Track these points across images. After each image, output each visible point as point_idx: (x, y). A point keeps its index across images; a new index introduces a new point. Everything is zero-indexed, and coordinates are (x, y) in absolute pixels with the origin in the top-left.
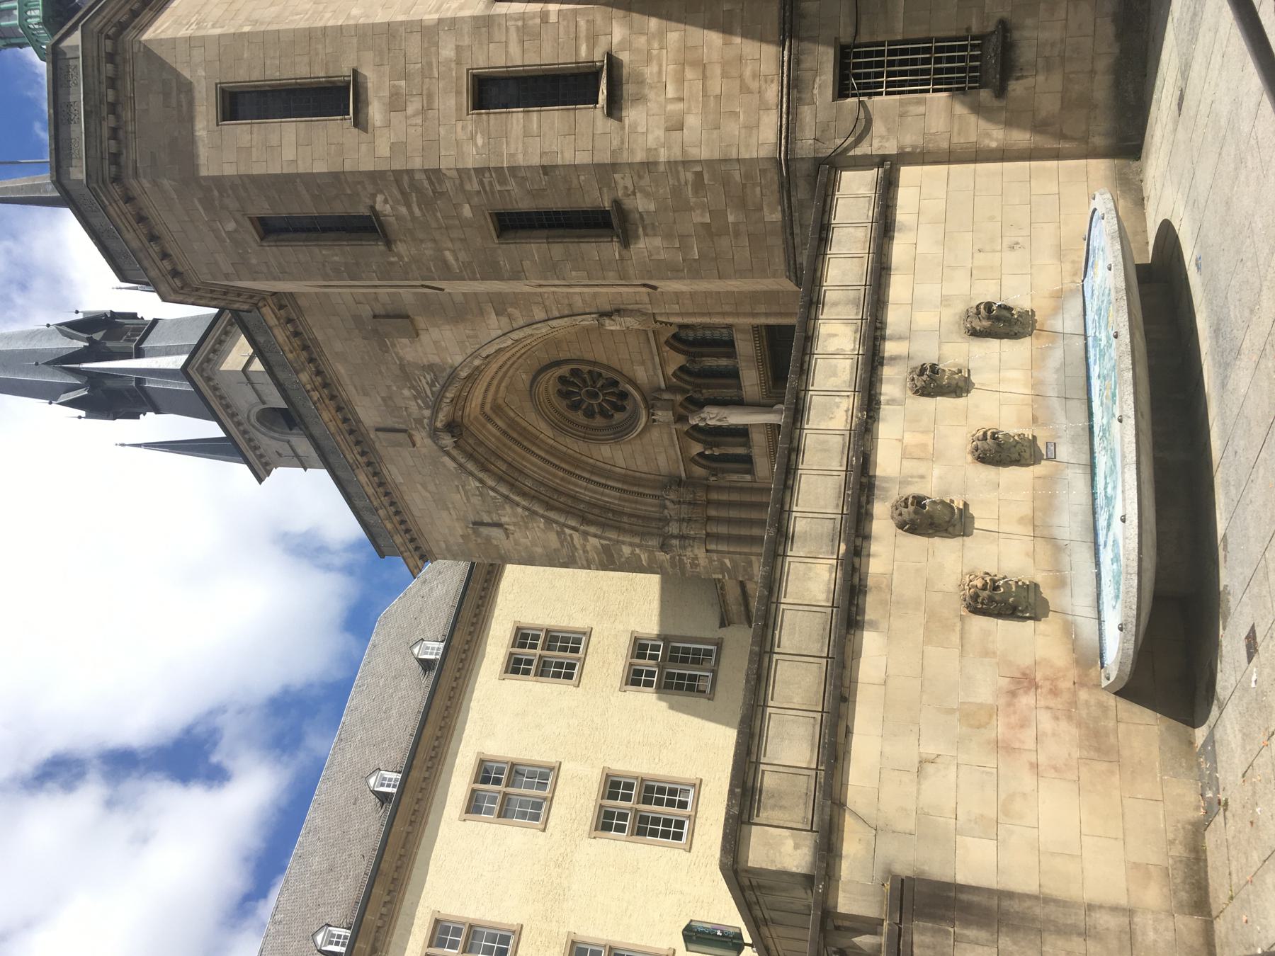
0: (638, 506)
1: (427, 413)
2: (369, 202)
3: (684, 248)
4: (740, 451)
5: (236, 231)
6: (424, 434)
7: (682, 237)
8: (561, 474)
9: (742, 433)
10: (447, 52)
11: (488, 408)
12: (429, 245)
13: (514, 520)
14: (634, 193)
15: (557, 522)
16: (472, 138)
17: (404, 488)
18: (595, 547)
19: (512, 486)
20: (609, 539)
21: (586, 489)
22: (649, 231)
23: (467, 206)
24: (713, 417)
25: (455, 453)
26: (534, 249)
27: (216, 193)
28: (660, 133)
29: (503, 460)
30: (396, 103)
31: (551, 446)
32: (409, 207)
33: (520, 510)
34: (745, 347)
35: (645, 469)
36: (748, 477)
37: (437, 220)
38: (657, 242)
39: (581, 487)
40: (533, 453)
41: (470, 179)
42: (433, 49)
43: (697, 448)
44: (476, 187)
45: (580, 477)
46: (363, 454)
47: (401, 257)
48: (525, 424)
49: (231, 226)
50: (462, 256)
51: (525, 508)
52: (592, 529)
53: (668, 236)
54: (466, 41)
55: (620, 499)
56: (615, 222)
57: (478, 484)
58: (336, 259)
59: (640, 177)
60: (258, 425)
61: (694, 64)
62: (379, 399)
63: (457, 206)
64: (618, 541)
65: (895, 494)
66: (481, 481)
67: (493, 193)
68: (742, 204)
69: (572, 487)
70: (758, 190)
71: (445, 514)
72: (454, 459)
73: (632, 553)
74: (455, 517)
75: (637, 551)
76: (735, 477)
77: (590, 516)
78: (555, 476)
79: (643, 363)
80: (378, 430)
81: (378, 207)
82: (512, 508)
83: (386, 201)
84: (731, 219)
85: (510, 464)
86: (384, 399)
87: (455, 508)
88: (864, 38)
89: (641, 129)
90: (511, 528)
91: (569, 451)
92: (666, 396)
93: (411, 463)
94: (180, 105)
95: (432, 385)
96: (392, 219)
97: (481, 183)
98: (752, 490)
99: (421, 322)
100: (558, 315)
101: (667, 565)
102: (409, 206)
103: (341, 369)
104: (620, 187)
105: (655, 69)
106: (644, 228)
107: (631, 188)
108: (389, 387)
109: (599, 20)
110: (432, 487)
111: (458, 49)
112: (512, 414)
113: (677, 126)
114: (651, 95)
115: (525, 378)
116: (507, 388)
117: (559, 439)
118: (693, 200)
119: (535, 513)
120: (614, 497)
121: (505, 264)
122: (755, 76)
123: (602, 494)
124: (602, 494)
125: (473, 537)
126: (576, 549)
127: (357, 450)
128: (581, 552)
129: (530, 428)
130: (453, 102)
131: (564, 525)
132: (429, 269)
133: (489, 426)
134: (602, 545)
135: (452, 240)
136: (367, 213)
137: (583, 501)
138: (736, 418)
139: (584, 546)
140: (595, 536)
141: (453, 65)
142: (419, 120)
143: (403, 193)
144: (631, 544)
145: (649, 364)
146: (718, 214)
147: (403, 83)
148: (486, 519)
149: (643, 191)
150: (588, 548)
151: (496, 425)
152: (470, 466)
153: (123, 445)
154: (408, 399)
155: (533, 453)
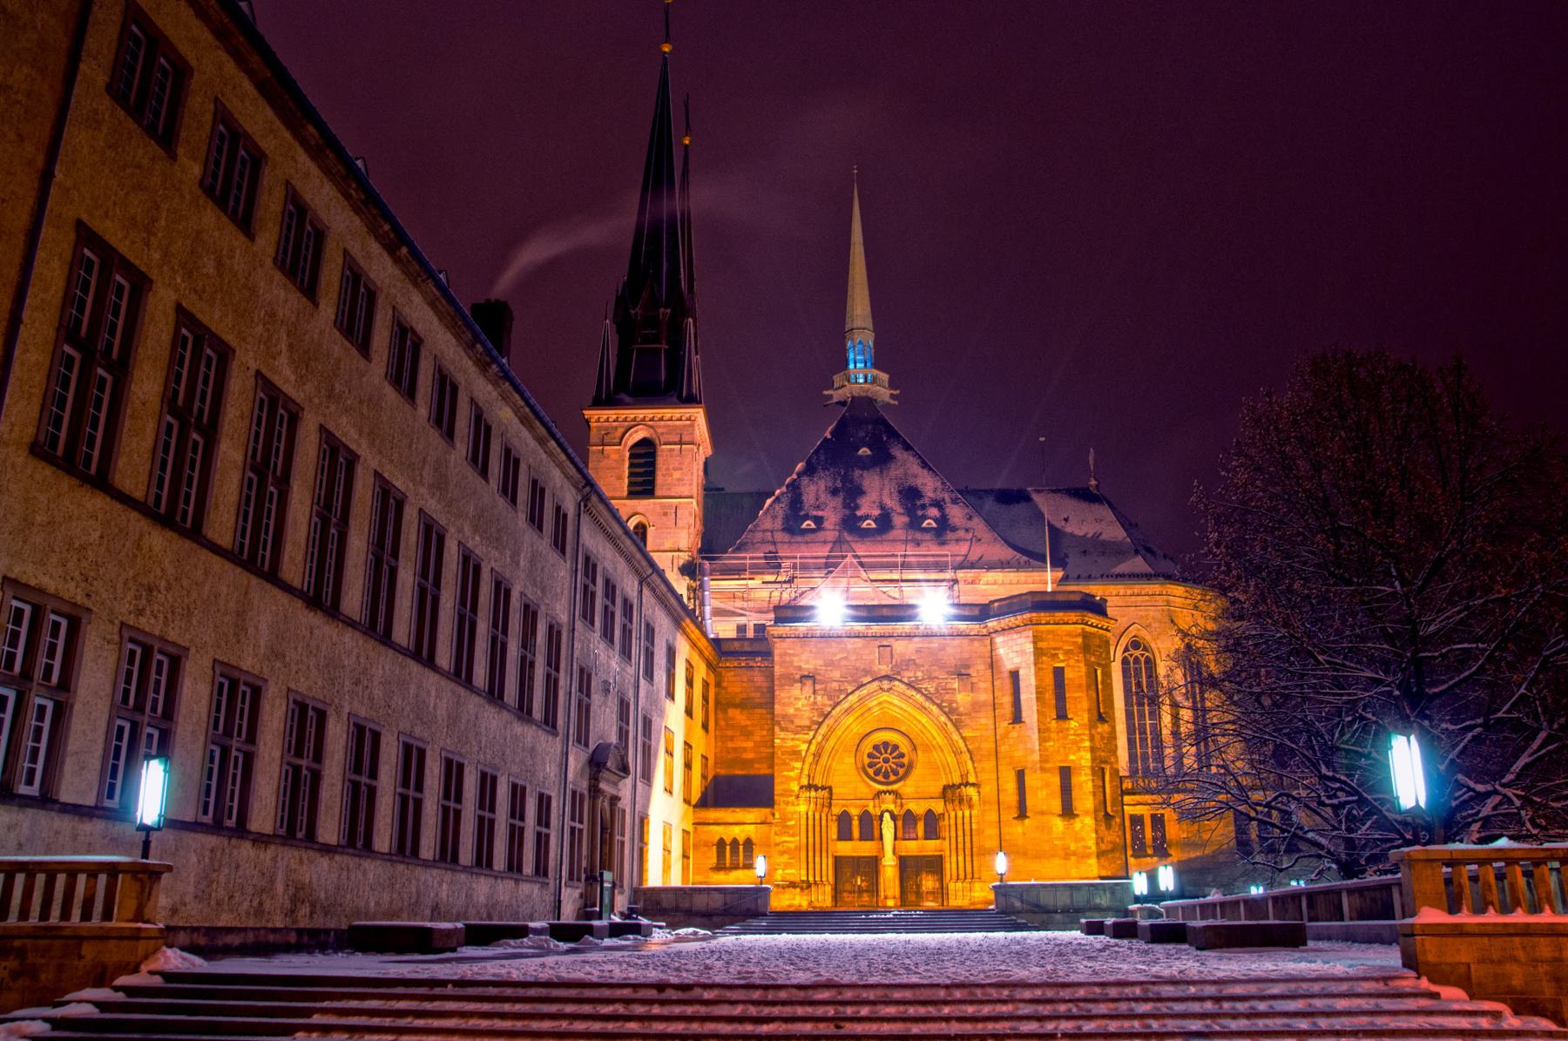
1: (905, 680)
13: (819, 703)
26: (1056, 780)
32: (1074, 735)
33: (829, 709)
34: (930, 847)
49: (1061, 657)
50: (1051, 749)
51: (830, 712)
52: (813, 748)
53: (1064, 833)
57: (849, 691)
63: (1074, 754)
71: (821, 662)
95: (926, 689)
101: (785, 786)
108: (923, 666)
110: (843, 663)
115: (903, 729)
119: (826, 716)
128: (792, 736)
133: (876, 702)
144: (802, 769)
148: (818, 687)
150: (797, 742)
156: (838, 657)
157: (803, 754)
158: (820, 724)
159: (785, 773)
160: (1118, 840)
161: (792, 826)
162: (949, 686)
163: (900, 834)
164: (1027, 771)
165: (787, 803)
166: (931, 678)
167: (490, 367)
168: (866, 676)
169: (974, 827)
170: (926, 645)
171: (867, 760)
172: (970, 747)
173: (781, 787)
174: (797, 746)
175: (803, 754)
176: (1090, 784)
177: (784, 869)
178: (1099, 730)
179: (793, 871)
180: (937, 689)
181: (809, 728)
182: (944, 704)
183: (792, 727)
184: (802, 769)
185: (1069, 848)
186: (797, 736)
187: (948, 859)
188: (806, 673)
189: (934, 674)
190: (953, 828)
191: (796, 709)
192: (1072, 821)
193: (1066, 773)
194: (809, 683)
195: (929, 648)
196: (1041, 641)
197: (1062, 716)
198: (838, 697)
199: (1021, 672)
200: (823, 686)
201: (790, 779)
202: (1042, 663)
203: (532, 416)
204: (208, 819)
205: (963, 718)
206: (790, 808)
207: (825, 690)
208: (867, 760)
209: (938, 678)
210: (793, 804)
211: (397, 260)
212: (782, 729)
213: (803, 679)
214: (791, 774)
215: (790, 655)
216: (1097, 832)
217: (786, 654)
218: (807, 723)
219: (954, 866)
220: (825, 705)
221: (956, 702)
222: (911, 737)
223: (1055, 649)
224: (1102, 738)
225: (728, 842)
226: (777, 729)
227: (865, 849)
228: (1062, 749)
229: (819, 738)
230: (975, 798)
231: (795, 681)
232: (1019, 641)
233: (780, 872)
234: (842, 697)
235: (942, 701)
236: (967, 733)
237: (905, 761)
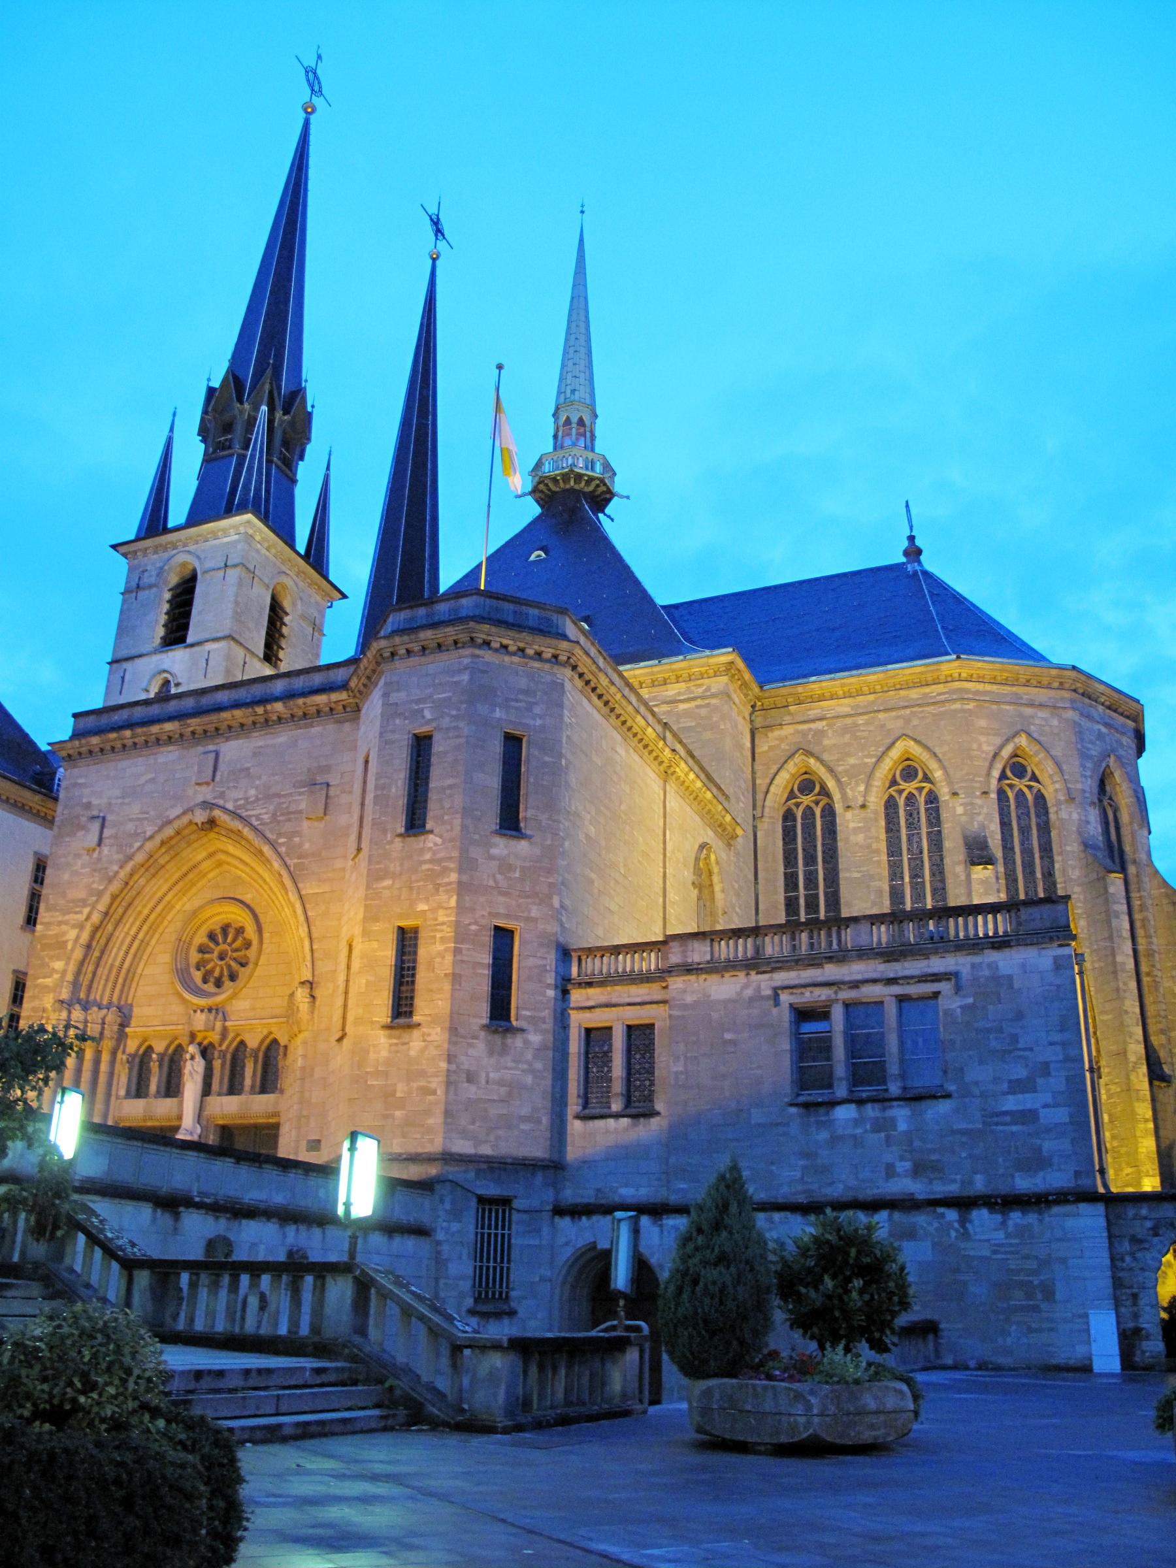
0: (102, 982)
1: (230, 806)
2: (436, 831)
3: (377, 1074)
4: (153, 1088)
5: (423, 717)
7: (386, 1074)
8: (146, 912)
9: (172, 1088)
10: (535, 912)
11: (223, 857)
13: (104, 859)
14: (424, 1041)
15: (97, 901)
16: (476, 923)
17: (151, 760)
18: (64, 934)
20: (73, 950)
21: (127, 933)
22: (394, 1048)
23: (426, 908)
25: (185, 820)
26: (388, 954)
27: (454, 713)
28: (466, 1067)
29: (169, 861)
30: (505, 866)
31: (173, 907)
32: (430, 861)
33: (116, 868)
35: (140, 993)
36: (122, 1092)
37: (417, 881)
38: (384, 1054)
39: (130, 929)
40: (170, 889)
41: (447, 915)
42: (537, 901)
44: (441, 919)
45: (140, 929)
46: (193, 733)
47: (391, 842)
48: (199, 885)
49: (428, 714)
50: (386, 893)
51: (117, 873)
52: (85, 937)
53: (388, 1062)
54: (541, 927)
55: (112, 966)
56: (402, 1021)
57: (149, 834)
58: (394, 790)
59: (436, 1047)
61: (510, 1094)
62: (249, 765)
63: (427, 900)
64: (69, 958)
65: (232, 1237)
66: (151, 837)
67: (436, 930)
69: (131, 920)
70: (418, 1136)
71: (117, 792)
72: (178, 817)
73: (54, 971)
74: (113, 801)
75: (56, 976)
76: (124, 1080)
77: (98, 935)
78: (144, 906)
79: (253, 1009)
80: (217, 754)
81: (431, 836)
83: (436, 844)
84: (398, 1113)
85: (163, 866)
86: (248, 769)
87: (122, 804)
88: (516, 1216)
89: (471, 1052)
90: (95, 855)
91: (165, 923)
92: (218, 1025)
93: (177, 776)
94: (517, 701)
95: (258, 818)
96: (421, 845)
97: (443, 924)
98: (108, 1094)
100: (315, 947)
101: (36, 1003)
102: (430, 861)
104: (430, 1031)
105: (510, 1064)
106: (396, 1044)
107: (429, 1039)
108: (259, 778)
109: (544, 1026)
110: (148, 788)
111: (535, 920)
112: (211, 875)
113: (471, 1078)
114: (492, 1061)
115: (247, 898)
116: (239, 877)
118: (415, 1085)
119: (110, 881)
120: (115, 959)
121: (376, 927)
122: (498, 1138)
123: (119, 949)
124: (119, 949)
125: (89, 814)
126: (64, 914)
127: (199, 729)
128: (60, 919)
129: (194, 890)
130: (502, 911)
131: (93, 908)
132: (378, 863)
133: (204, 854)
134: (67, 941)
135: (401, 888)
136: (428, 827)
137: (115, 929)
138: (191, 1088)
139: (66, 923)
140: (78, 937)
141: (525, 914)
142: (491, 883)
143: (439, 861)
144: (64, 972)
147: (517, 875)
148: (107, 832)
149: (426, 1047)
150: (64, 928)
151: (204, 859)
152: (169, 831)
153: (174, 415)
154: (246, 792)
155: (170, 889)
158: (100, 894)
159: (41, 981)
160: (529, 1080)
162: (293, 808)
166: (268, 797)
168: (172, 807)
170: (270, 742)
171: (194, 957)
176: (449, 958)
178: (494, 851)
180: (274, 815)
181: (84, 903)
182: (281, 840)
186: (67, 917)
189: (273, 790)
191: (76, 873)
192: (406, 1036)
193: (407, 941)
196: (398, 690)
197: (415, 822)
198: (131, 846)
201: (46, 989)
202: (393, 731)
208: (194, 957)
209: (278, 796)
214: (48, 981)
215: (80, 784)
216: (450, 1058)
217: (75, 785)
218: (81, 894)
221: (297, 833)
222: (258, 910)
223: (417, 702)
228: (405, 892)
234: (137, 845)
235: (280, 835)
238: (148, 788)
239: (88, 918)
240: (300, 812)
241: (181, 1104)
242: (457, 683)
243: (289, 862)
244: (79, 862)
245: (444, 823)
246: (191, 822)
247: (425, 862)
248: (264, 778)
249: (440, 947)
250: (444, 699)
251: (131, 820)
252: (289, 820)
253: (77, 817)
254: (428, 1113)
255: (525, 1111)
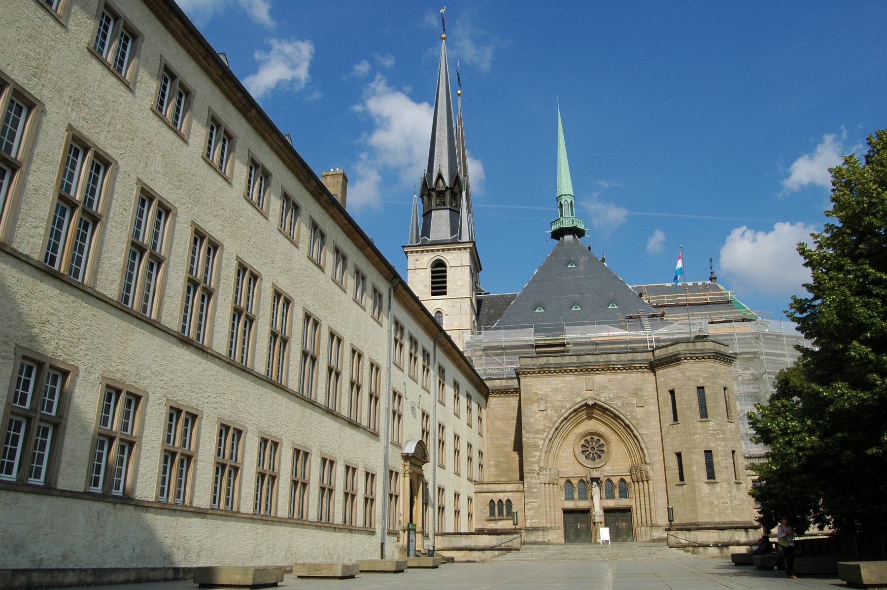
1: (603, 399)
6: (592, 395)
7: (709, 497)
12: (701, 432)
13: (549, 415)
15: (550, 430)
17: (562, 378)
18: (538, 442)
19: (566, 418)
24: (596, 490)
25: (584, 402)
26: (703, 460)
33: (556, 419)
34: (623, 503)
36: (562, 499)
38: (707, 491)
43: (575, 482)
50: (698, 440)
52: (547, 442)
53: (709, 494)
57: (568, 407)
60: (436, 258)
63: (713, 442)
68: (720, 513)
71: (549, 390)
82: (556, 416)
84: (716, 510)
92: (602, 476)
93: (576, 386)
95: (616, 404)
99: (643, 409)
101: (530, 467)
103: (620, 376)
108: (613, 390)
110: (563, 389)
117: (573, 435)
118: (720, 501)
119: (555, 423)
121: (697, 450)
126: (535, 435)
131: (549, 433)
139: (538, 438)
140: (544, 443)
143: (716, 430)
144: (540, 456)
145: (613, 471)
146: (717, 506)
148: (548, 405)
150: (537, 440)
152: (577, 406)
156: (560, 386)
157: (541, 447)
158: (551, 428)
160: (745, 498)
161: (536, 492)
162: (630, 402)
163: (604, 496)
164: (682, 454)
165: (532, 478)
166: (619, 398)
167: (322, 197)
169: (651, 490)
172: (645, 440)
173: (527, 468)
174: (537, 442)
175: (541, 447)
177: (531, 520)
178: (728, 427)
179: (537, 521)
180: (622, 404)
181: (544, 431)
182: (628, 414)
183: (533, 430)
184: (540, 456)
185: (713, 503)
186: (537, 436)
187: (635, 512)
188: (540, 397)
189: (620, 395)
190: (637, 491)
191: (535, 419)
192: (714, 486)
194: (543, 402)
195: (616, 379)
196: (688, 371)
199: (676, 392)
200: (551, 404)
201: (534, 463)
202: (689, 385)
203: (354, 231)
204: (99, 489)
205: (640, 422)
206: (534, 481)
207: (553, 407)
210: (536, 479)
211: (249, 120)
212: (527, 432)
213: (539, 401)
217: (528, 385)
218: (542, 427)
219: (639, 515)
220: (553, 416)
223: (697, 376)
224: (731, 432)
225: (496, 503)
226: (523, 432)
227: (583, 504)
229: (550, 436)
230: (650, 473)
231: (536, 402)
232: (674, 372)
233: (529, 521)
234: (564, 411)
235: (627, 412)
236: (642, 431)
237: (605, 449)
238: (563, 389)
239: (547, 437)
240: (634, 404)
241: (600, 504)
242: (710, 372)
243: (632, 421)
244: (538, 415)
245: (715, 418)
246: (586, 404)
247: (711, 430)
248: (615, 390)
249: (720, 458)
250: (706, 377)
251: (559, 401)
252: (630, 406)
253: (532, 397)
254: (726, 509)
255: (745, 507)
